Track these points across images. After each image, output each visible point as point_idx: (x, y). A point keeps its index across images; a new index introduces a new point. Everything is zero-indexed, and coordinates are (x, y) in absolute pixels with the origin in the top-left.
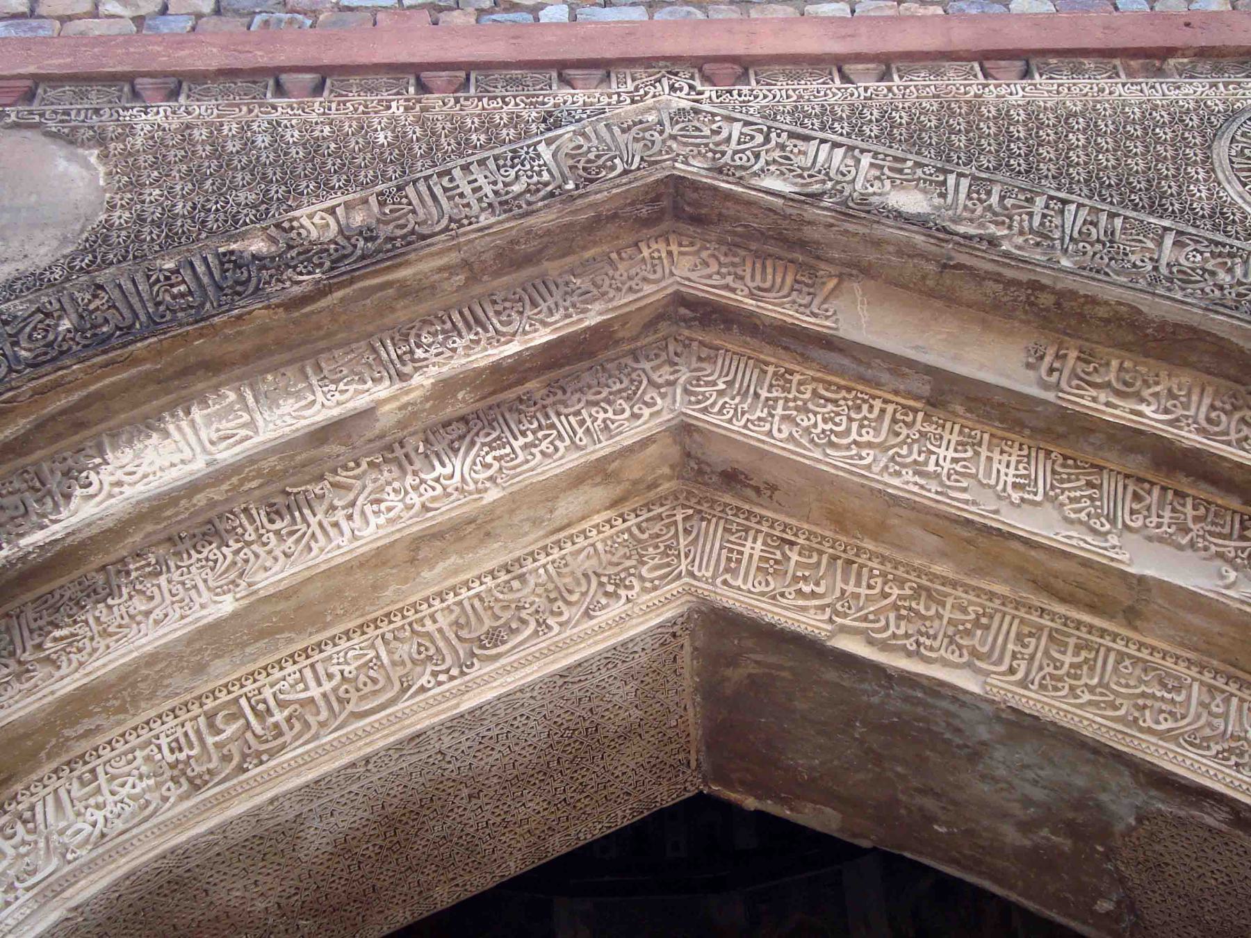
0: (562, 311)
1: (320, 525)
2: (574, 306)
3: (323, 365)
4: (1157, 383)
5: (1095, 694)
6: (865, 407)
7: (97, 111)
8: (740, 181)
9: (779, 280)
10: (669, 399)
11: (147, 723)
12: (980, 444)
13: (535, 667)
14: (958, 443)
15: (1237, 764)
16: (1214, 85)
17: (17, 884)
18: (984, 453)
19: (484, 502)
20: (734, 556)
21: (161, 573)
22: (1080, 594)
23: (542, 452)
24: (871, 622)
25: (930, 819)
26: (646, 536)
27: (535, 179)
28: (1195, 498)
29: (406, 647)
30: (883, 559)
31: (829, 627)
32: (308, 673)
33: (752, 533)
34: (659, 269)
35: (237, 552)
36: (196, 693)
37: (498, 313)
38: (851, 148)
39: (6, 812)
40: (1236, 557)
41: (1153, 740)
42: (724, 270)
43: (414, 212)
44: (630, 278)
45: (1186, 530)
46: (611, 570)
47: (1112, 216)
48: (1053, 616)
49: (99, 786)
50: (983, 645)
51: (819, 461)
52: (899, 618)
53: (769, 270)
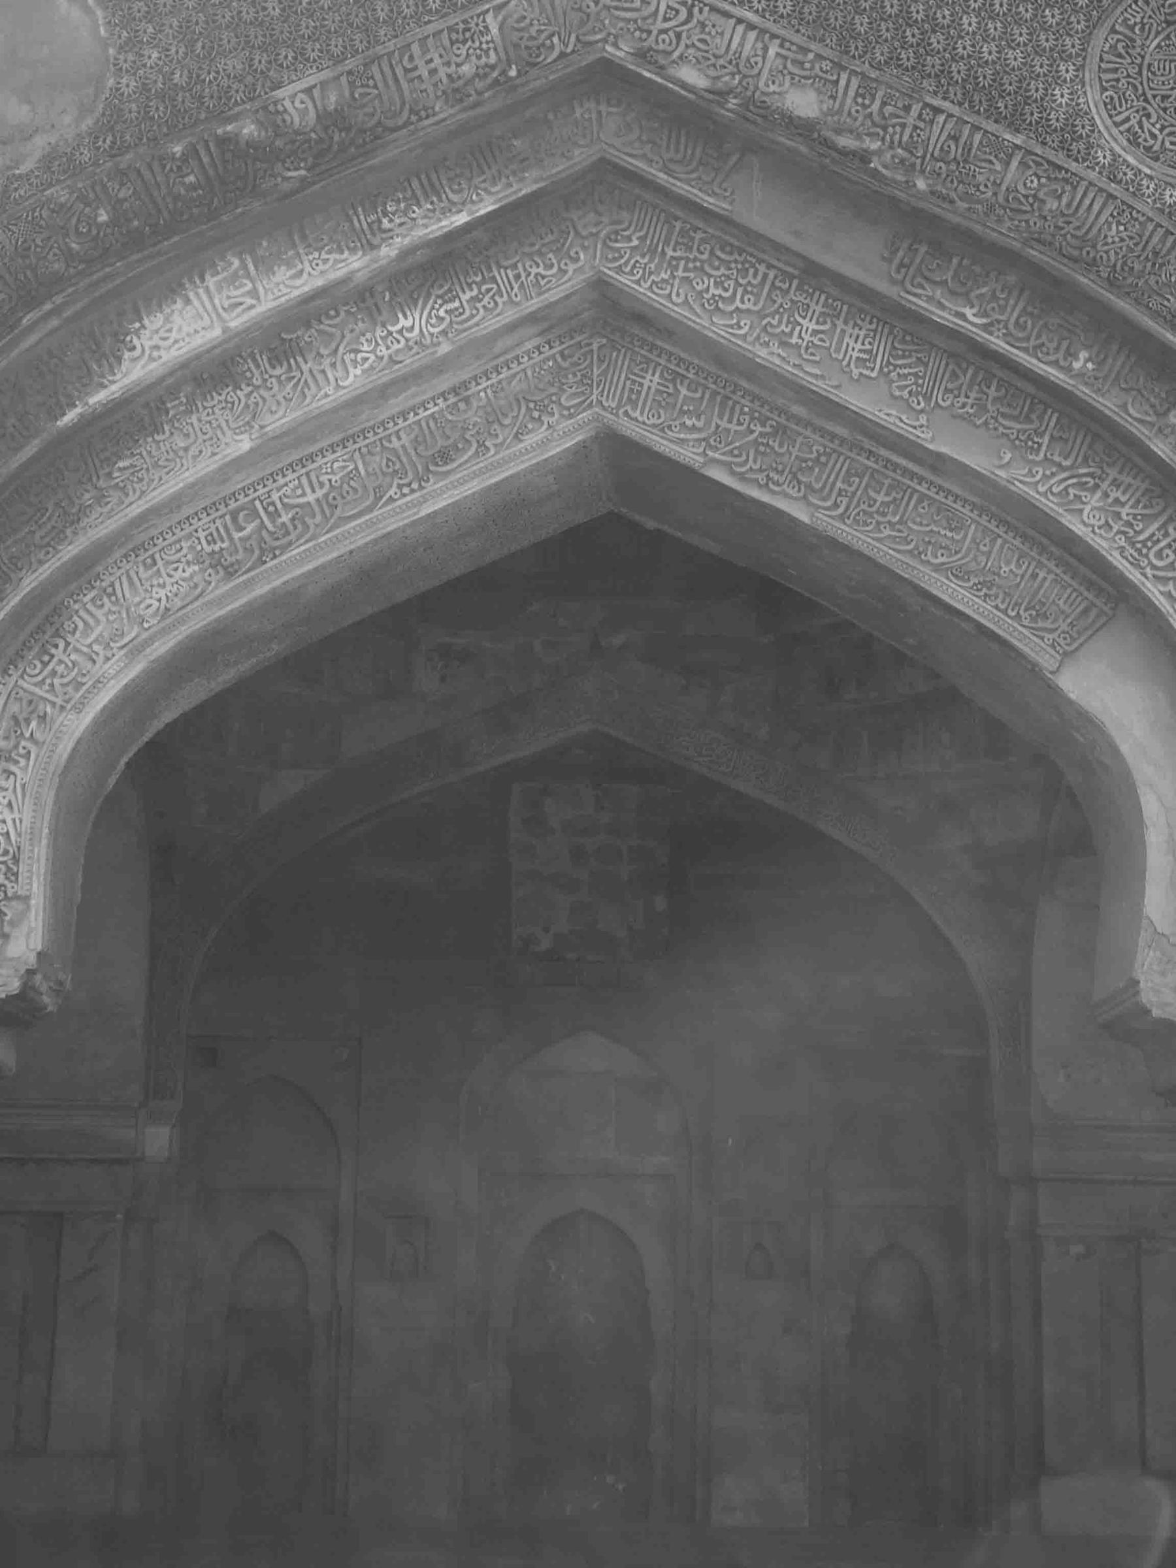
1: (311, 371)
2: (514, 173)
4: (985, 284)
5: (893, 530)
6: (751, 271)
8: (660, 69)
9: (690, 152)
10: (591, 251)
11: (188, 518)
12: (838, 318)
14: (822, 314)
15: (986, 595)
17: (112, 644)
18: (840, 324)
19: (439, 354)
21: (192, 412)
23: (484, 307)
24: (736, 456)
28: (1001, 379)
29: (378, 458)
30: (755, 398)
32: (304, 480)
36: (221, 496)
37: (449, 179)
38: (763, 31)
39: (93, 588)
40: (1017, 438)
45: (983, 409)
48: (877, 458)
49: (158, 570)
53: (683, 140)
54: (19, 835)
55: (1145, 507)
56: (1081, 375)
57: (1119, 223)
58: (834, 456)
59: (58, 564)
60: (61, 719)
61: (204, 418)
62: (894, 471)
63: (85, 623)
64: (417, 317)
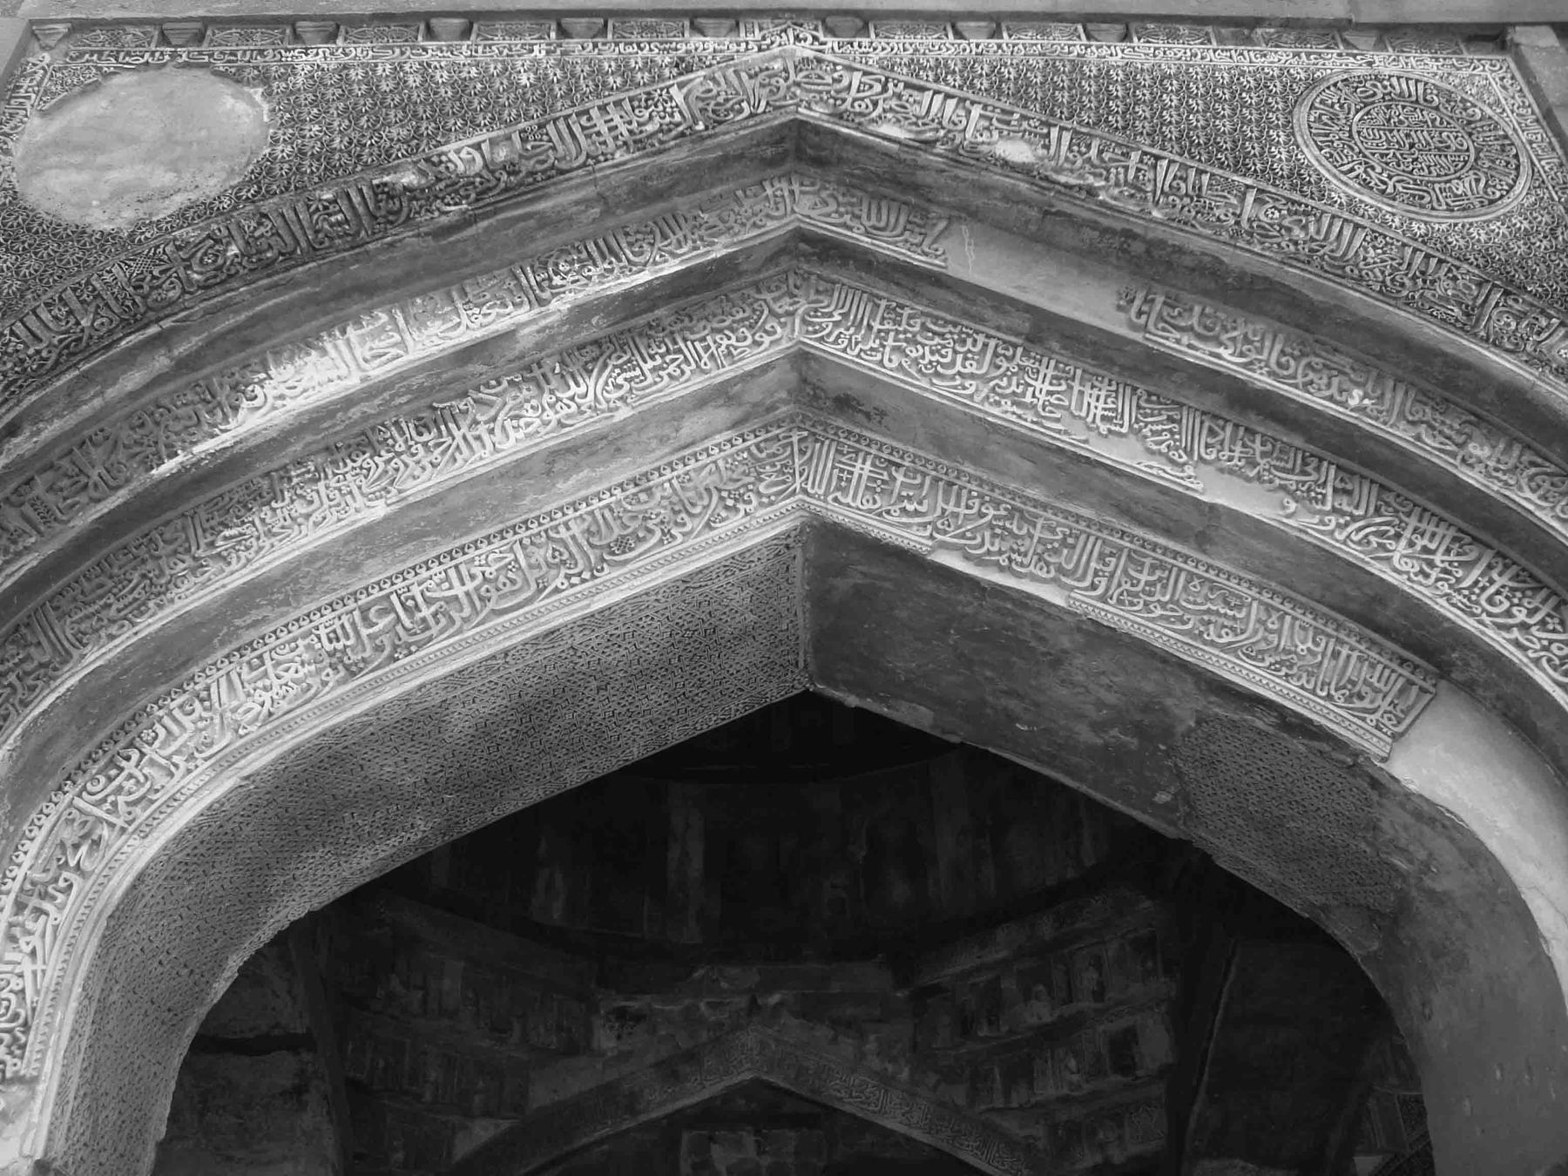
0: (690, 243)
1: (464, 437)
2: (702, 239)
3: (468, 289)
4: (1235, 329)
6: (969, 341)
7: (261, 52)
8: (859, 127)
9: (892, 220)
10: (788, 329)
12: (1073, 379)
13: (660, 572)
14: (1054, 377)
16: (1297, 55)
18: (1077, 387)
19: (615, 420)
20: (845, 475)
22: (1158, 519)
23: (669, 375)
25: (1012, 718)
26: (763, 455)
27: (668, 119)
29: (542, 552)
30: (981, 483)
31: (930, 543)
32: (452, 573)
33: (861, 455)
34: (781, 206)
35: (388, 461)
36: (351, 590)
37: (631, 245)
38: (962, 100)
41: (1216, 652)
42: (842, 209)
43: (554, 148)
44: (755, 215)
45: (1253, 464)
46: (731, 486)
47: (1200, 172)
48: (1132, 538)
50: (1068, 562)
51: (926, 390)
52: (994, 536)
53: (884, 212)
54: (37, 992)
55: (1458, 554)
56: (1361, 409)
57: (1375, 248)
58: (1083, 537)
59: (135, 639)
60: (119, 843)
61: (333, 483)
62: (1154, 550)
63: (169, 732)
64: (591, 383)
